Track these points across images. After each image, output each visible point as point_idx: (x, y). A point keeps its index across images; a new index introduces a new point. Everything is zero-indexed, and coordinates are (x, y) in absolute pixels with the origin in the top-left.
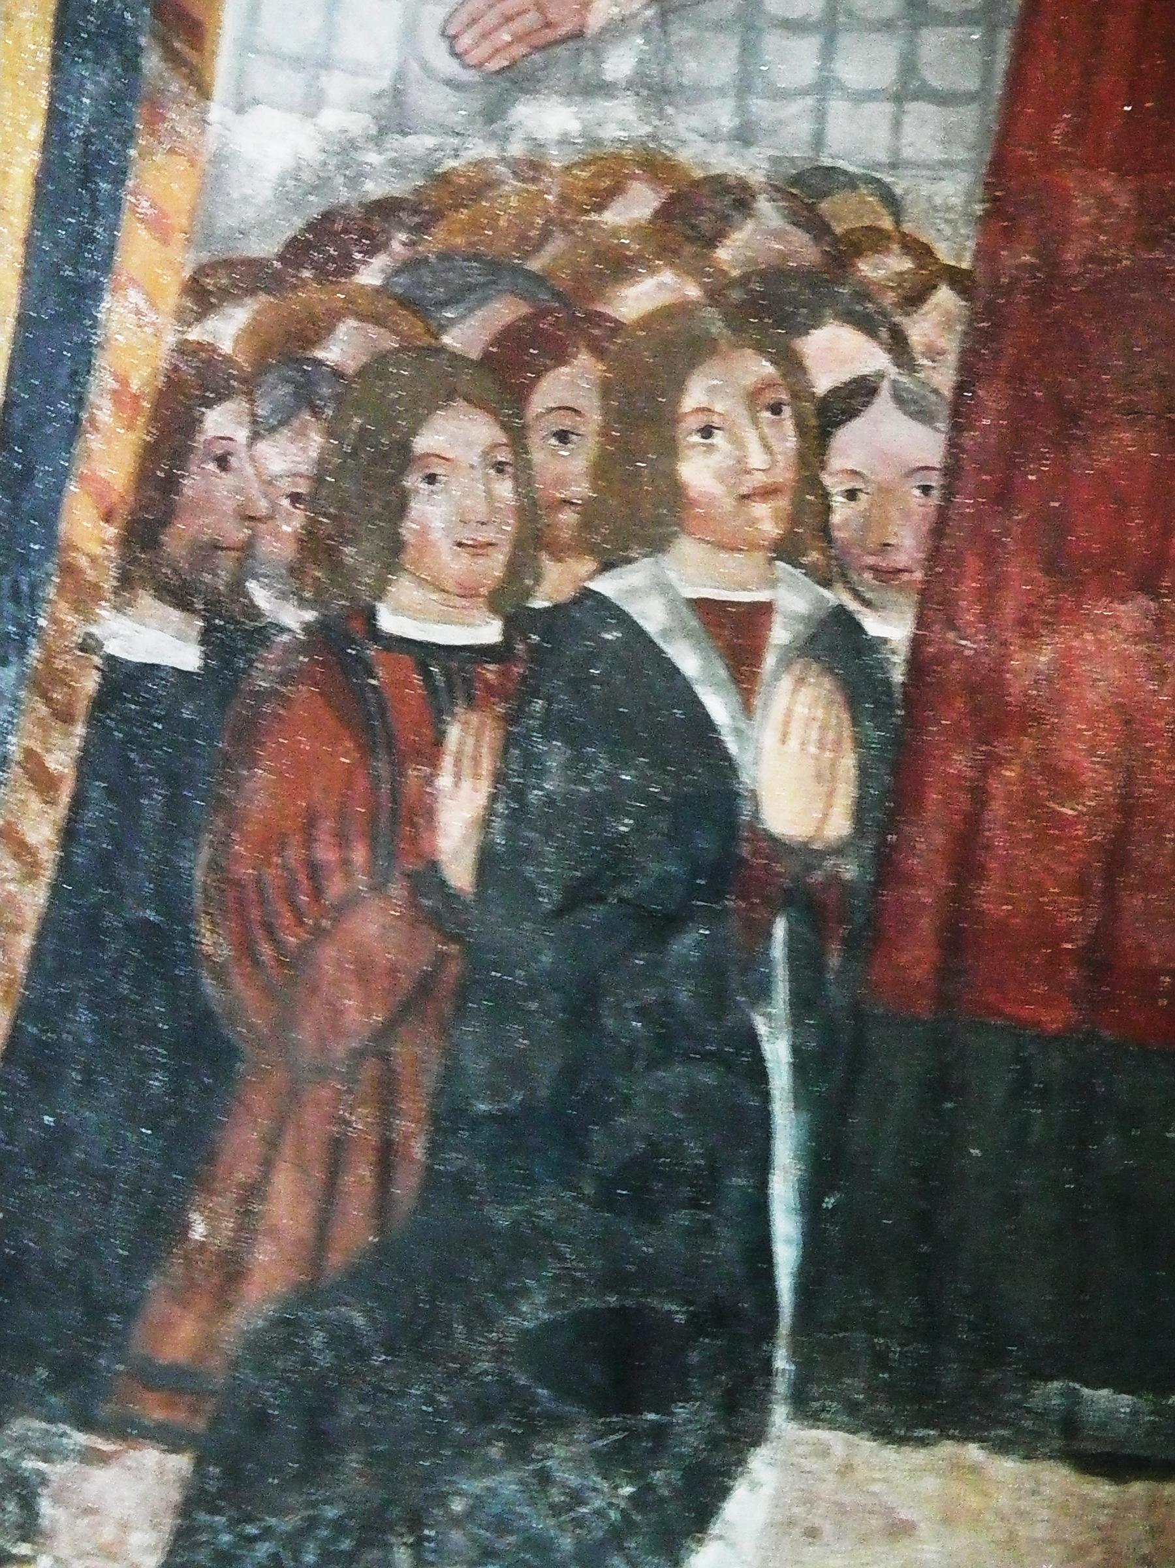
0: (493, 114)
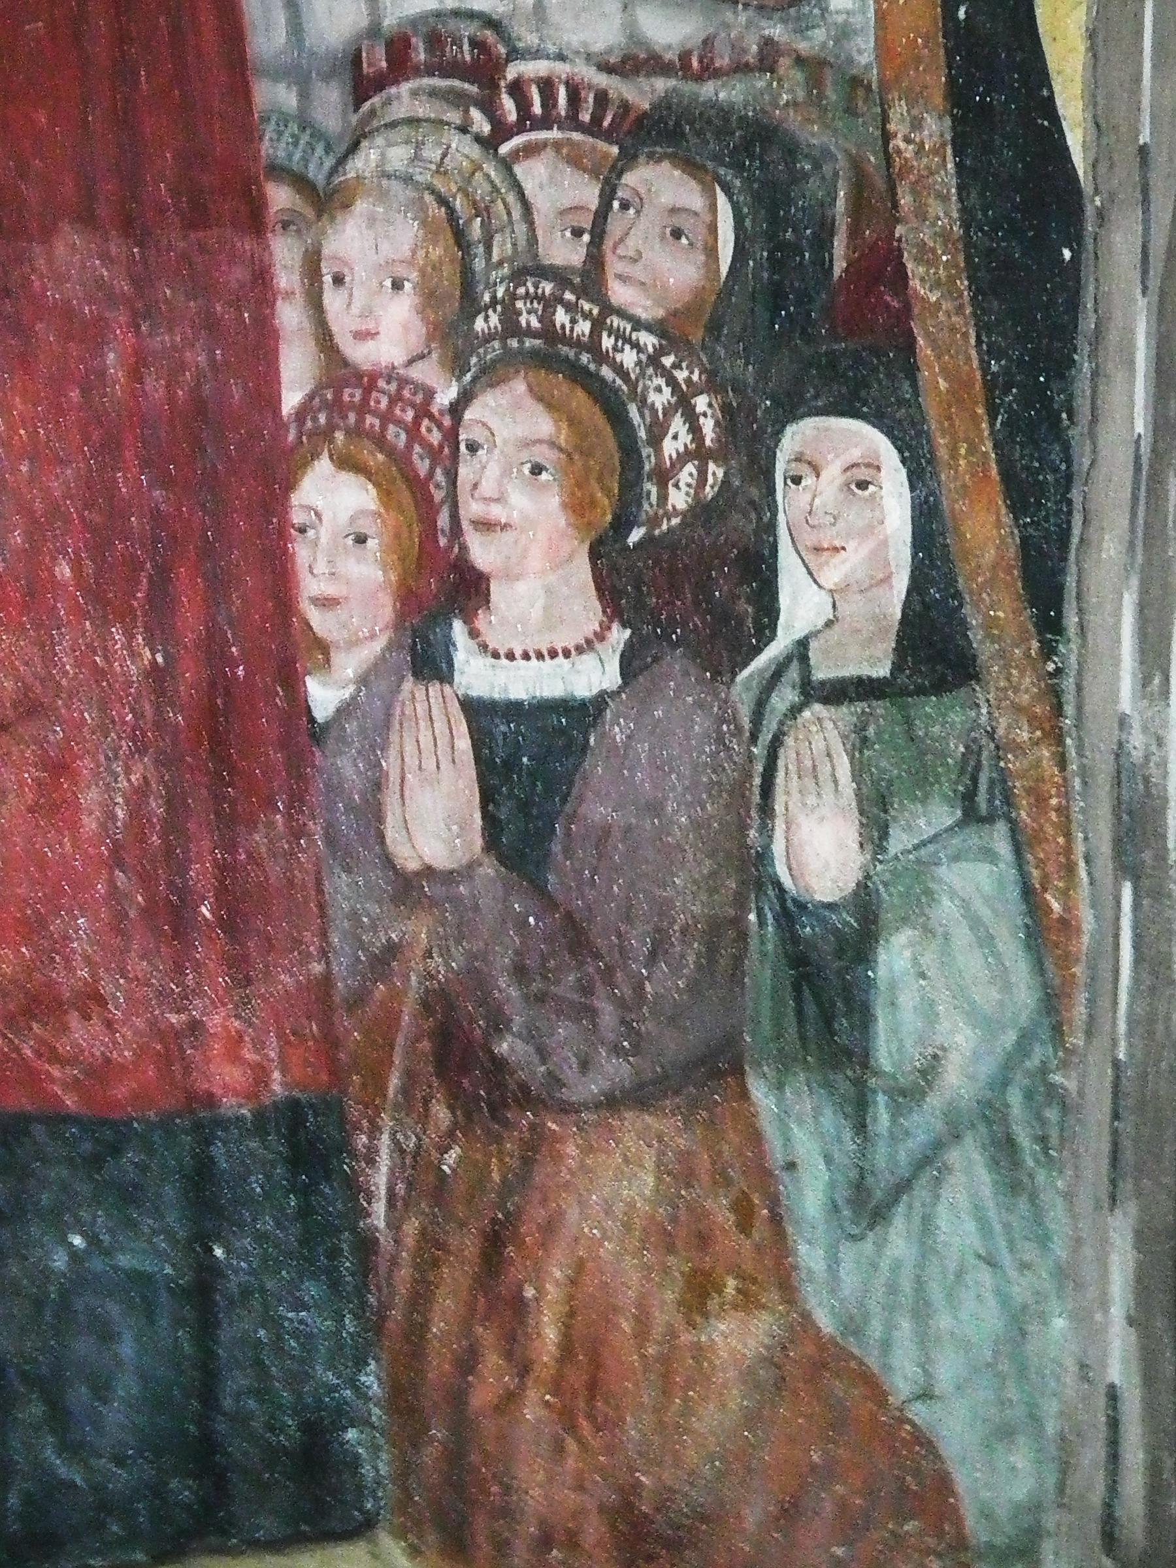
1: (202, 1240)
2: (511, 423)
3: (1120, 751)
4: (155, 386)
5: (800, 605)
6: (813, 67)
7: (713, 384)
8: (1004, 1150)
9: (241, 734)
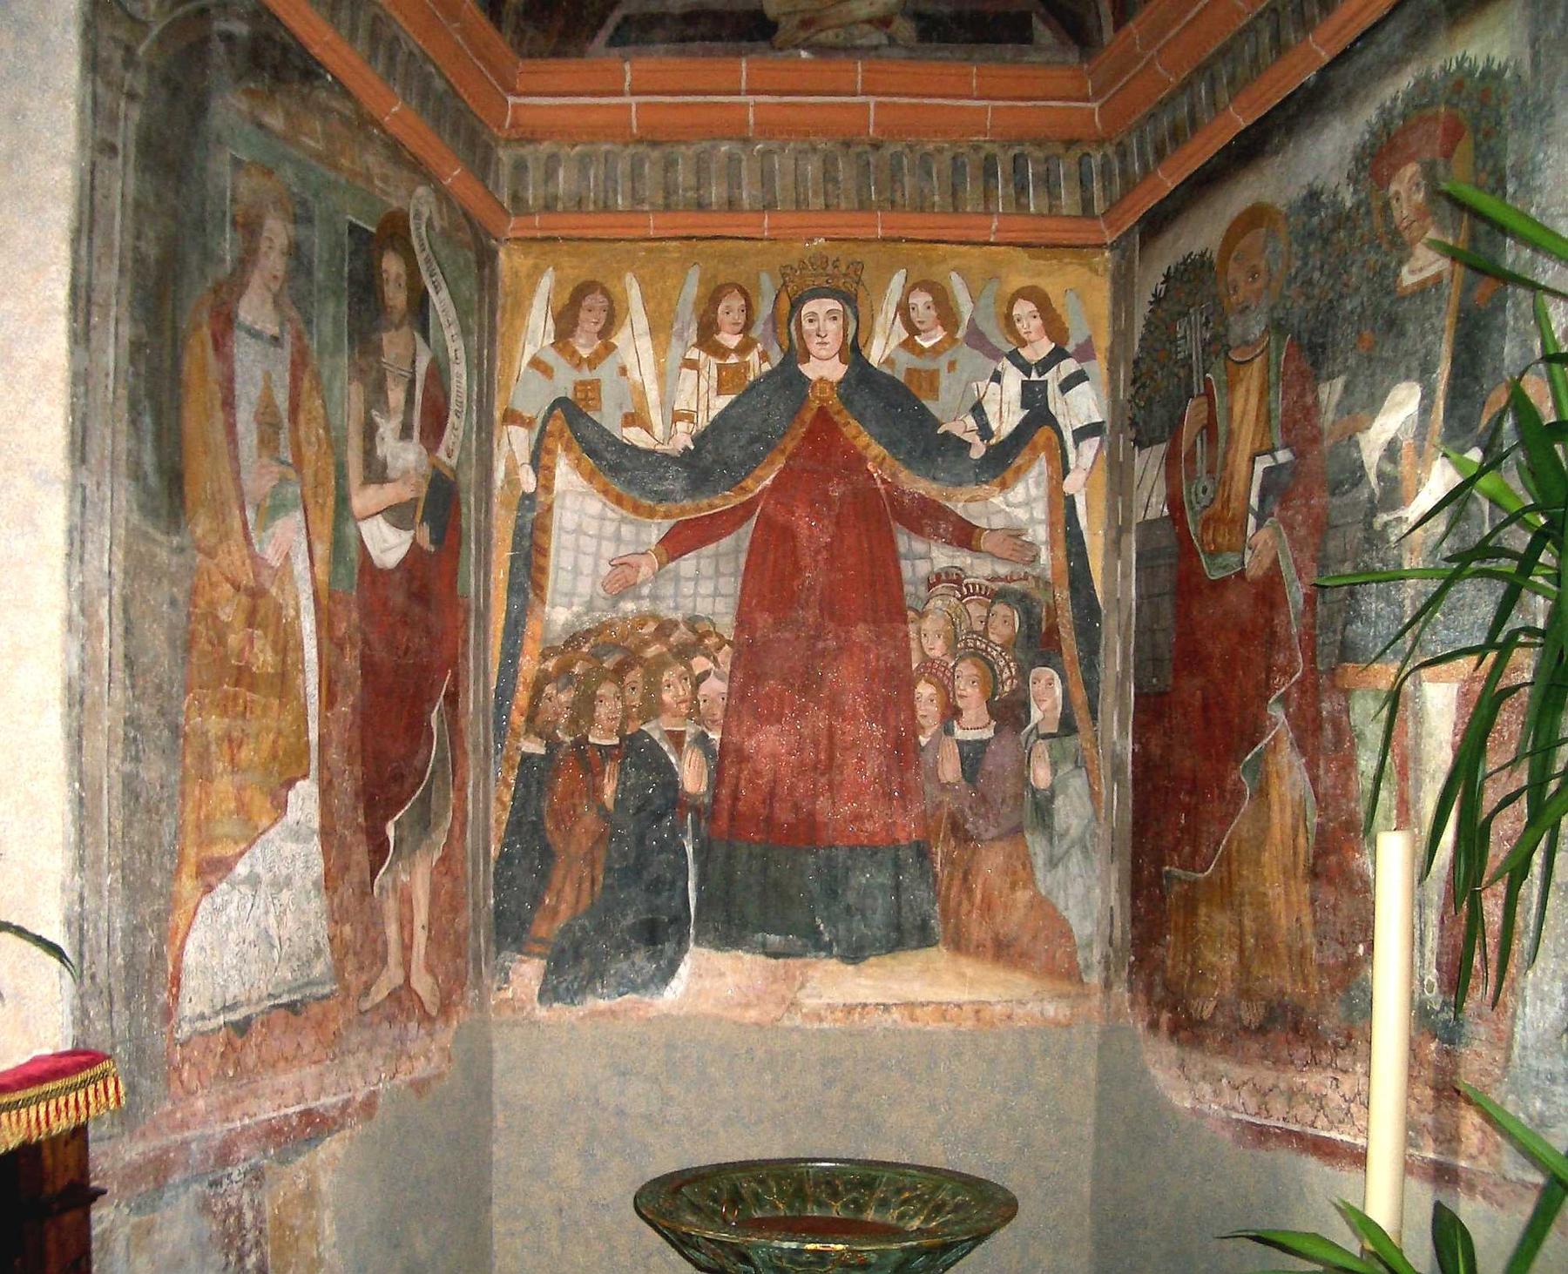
0: (614, 606)
1: (897, 875)
2: (966, 670)
3: (1114, 751)
4: (882, 663)
5: (1036, 715)
6: (1037, 579)
7: (1014, 660)
8: (1084, 849)
9: (903, 750)
